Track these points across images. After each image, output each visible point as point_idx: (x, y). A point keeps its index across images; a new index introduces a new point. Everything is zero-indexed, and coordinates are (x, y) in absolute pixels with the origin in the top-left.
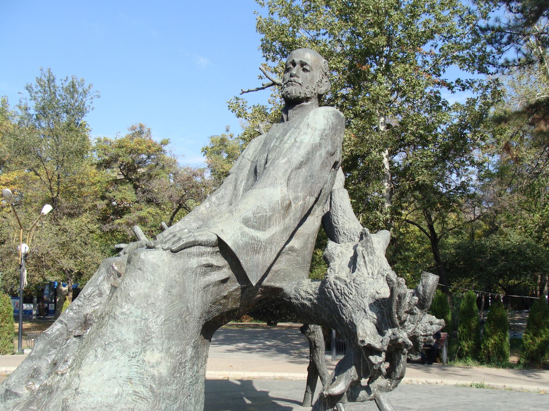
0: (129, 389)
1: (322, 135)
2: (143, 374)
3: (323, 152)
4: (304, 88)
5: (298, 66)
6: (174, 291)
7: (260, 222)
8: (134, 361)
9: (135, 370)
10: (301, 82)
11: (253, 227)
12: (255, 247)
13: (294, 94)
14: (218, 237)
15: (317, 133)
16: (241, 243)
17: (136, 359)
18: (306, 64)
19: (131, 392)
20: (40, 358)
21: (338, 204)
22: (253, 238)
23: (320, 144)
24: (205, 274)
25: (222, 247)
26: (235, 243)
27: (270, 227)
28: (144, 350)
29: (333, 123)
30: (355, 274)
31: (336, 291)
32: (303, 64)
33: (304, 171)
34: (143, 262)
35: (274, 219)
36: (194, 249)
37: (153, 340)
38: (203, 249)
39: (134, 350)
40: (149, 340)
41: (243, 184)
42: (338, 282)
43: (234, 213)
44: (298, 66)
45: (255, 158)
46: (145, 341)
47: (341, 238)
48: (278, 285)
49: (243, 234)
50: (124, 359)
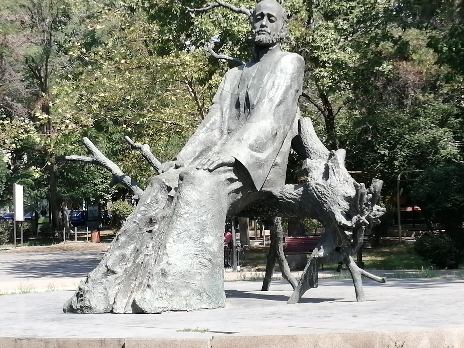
0: (196, 261)
1: (292, 78)
2: (203, 251)
3: (293, 91)
4: (272, 36)
5: (266, 18)
6: (215, 197)
7: (258, 147)
8: (197, 243)
9: (199, 249)
10: (269, 31)
11: (255, 151)
12: (259, 164)
13: (265, 42)
14: (236, 159)
15: (288, 76)
16: (251, 162)
17: (198, 242)
18: (272, 16)
19: (198, 262)
20: (124, 248)
21: (306, 130)
22: (257, 158)
23: (291, 85)
24: (228, 185)
25: (237, 166)
26: (248, 163)
27: (266, 150)
28: (203, 236)
29: (298, 67)
30: (329, 181)
31: (317, 193)
32: (269, 16)
33: (282, 108)
34: (194, 178)
35: (267, 144)
36: (222, 169)
37: (207, 229)
38: (227, 168)
39: (196, 236)
40: (205, 229)
41: (227, 113)
42: (318, 186)
43: (242, 141)
44: (266, 18)
45: (234, 91)
46: (203, 230)
47: (312, 156)
48: (269, 190)
49: (252, 156)
50: (191, 242)
